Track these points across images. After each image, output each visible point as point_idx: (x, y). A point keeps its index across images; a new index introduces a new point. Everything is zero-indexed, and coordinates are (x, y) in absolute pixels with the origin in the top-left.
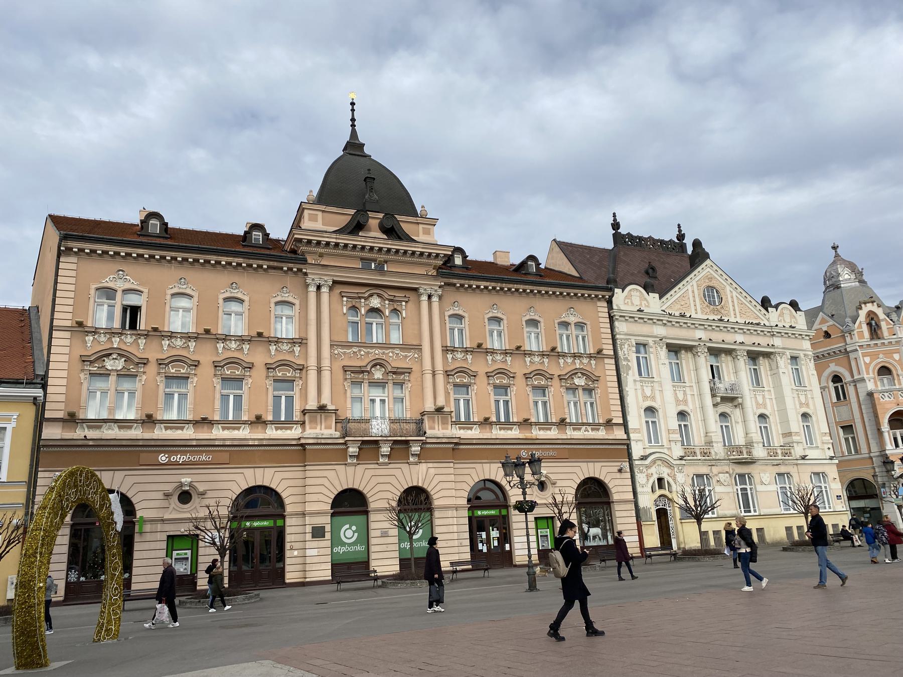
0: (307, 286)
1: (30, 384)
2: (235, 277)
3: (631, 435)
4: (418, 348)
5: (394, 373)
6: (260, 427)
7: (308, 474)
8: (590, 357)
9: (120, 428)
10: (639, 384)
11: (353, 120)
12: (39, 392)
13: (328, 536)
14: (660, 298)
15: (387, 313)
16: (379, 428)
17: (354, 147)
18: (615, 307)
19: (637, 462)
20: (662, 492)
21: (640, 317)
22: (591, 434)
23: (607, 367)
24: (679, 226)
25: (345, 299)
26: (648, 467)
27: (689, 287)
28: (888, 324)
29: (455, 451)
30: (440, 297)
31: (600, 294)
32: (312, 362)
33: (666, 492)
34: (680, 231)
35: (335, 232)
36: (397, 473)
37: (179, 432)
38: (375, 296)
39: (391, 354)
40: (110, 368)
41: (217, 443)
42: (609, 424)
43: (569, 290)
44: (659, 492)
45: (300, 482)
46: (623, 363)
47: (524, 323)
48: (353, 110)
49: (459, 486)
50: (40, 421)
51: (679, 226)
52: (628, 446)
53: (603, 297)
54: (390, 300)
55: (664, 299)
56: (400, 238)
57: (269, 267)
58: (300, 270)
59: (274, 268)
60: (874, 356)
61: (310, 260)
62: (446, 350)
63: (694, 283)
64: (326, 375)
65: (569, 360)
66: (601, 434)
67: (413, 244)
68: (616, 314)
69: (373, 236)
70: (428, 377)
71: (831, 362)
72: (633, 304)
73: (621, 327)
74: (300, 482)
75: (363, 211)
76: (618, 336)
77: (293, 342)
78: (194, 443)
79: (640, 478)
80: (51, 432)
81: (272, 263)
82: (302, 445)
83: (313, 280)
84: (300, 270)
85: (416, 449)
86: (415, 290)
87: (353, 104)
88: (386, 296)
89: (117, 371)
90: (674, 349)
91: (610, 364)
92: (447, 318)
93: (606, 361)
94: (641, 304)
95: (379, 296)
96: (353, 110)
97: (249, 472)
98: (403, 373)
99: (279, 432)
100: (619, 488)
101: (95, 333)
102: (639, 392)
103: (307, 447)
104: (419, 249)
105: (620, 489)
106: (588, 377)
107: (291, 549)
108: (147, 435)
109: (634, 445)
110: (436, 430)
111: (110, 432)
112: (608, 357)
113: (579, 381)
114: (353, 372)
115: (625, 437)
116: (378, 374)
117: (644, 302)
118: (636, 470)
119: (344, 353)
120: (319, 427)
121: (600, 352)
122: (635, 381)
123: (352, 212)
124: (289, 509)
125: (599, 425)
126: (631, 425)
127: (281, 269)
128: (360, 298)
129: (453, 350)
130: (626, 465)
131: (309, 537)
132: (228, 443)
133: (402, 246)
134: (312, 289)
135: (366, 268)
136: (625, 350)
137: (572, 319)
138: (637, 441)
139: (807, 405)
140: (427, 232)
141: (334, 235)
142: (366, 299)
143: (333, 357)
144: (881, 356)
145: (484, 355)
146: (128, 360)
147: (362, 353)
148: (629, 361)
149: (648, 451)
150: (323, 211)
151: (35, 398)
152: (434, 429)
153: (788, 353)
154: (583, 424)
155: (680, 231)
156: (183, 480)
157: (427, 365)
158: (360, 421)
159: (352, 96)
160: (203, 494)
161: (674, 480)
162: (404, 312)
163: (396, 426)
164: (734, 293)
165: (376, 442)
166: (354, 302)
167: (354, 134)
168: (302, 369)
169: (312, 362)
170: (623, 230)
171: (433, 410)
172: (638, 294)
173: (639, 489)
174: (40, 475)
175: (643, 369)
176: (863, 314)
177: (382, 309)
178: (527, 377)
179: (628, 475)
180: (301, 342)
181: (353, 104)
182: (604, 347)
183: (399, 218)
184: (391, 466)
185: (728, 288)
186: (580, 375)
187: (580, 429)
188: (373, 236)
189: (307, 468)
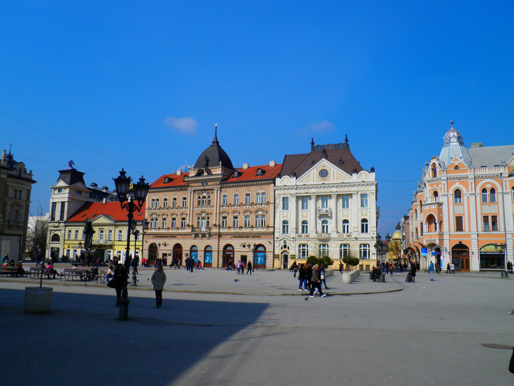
2: (174, 193)
20: (285, 249)
21: (285, 187)
24: (346, 135)
26: (280, 240)
27: (312, 172)
28: (439, 169)
33: (286, 249)
34: (346, 138)
42: (268, 227)
44: (284, 249)
46: (276, 205)
51: (346, 135)
55: (298, 179)
60: (432, 186)
63: (315, 170)
70: (215, 215)
71: (457, 182)
79: (277, 244)
90: (298, 198)
91: (272, 206)
100: (269, 248)
109: (276, 234)
130: (272, 242)
135: (203, 185)
139: (366, 215)
144: (435, 186)
153: (360, 193)
155: (346, 138)
159: (216, 125)
164: (335, 170)
169: (188, 213)
175: (285, 207)
176: (431, 163)
185: (332, 169)
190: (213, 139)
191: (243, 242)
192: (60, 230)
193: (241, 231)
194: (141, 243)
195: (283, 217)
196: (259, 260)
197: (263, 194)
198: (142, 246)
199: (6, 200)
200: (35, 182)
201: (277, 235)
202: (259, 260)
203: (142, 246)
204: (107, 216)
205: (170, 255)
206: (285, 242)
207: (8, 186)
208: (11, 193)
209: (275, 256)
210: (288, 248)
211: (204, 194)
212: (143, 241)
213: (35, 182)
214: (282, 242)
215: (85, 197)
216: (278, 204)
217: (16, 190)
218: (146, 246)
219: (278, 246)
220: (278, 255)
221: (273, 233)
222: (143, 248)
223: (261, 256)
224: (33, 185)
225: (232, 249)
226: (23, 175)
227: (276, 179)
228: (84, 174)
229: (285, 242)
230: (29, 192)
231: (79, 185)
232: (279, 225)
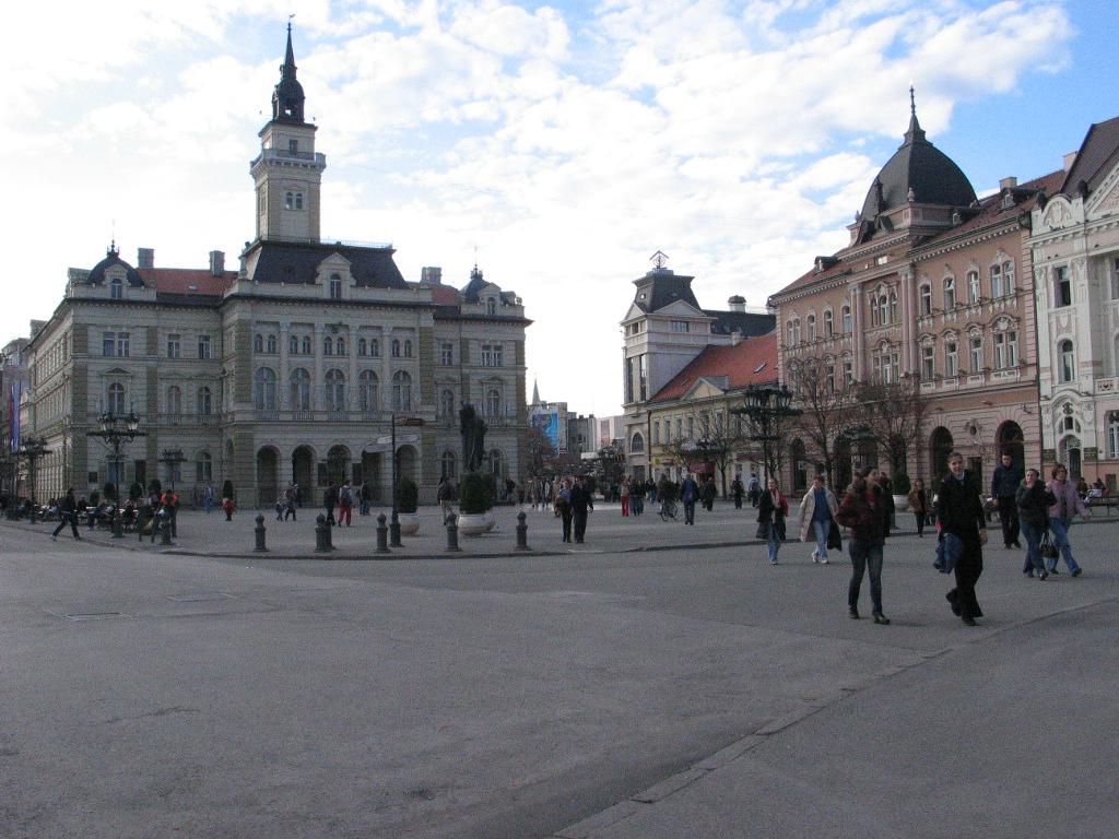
3: (1042, 376)
11: (913, 106)
14: (1084, 202)
20: (1070, 432)
26: (1056, 405)
33: (1073, 432)
42: (1023, 366)
44: (1066, 432)
48: (913, 97)
79: (1047, 419)
96: (913, 97)
109: (1042, 383)
142: (878, 291)
159: (911, 83)
161: (1082, 418)
167: (915, 121)
179: (1037, 416)
181: (912, 90)
190: (906, 127)
191: (969, 419)
192: (642, 424)
193: (963, 387)
195: (1059, 331)
199: (465, 371)
200: (529, 322)
201: (1045, 389)
204: (717, 381)
206: (1068, 410)
207: (467, 340)
208: (475, 353)
210: (1079, 431)
211: (884, 291)
213: (529, 322)
214: (1061, 409)
215: (703, 337)
217: (486, 347)
219: (1052, 420)
220: (1053, 451)
221: (1037, 382)
224: (527, 330)
226: (501, 312)
228: (690, 279)
229: (1068, 410)
230: (519, 347)
231: (678, 308)
232: (1048, 357)
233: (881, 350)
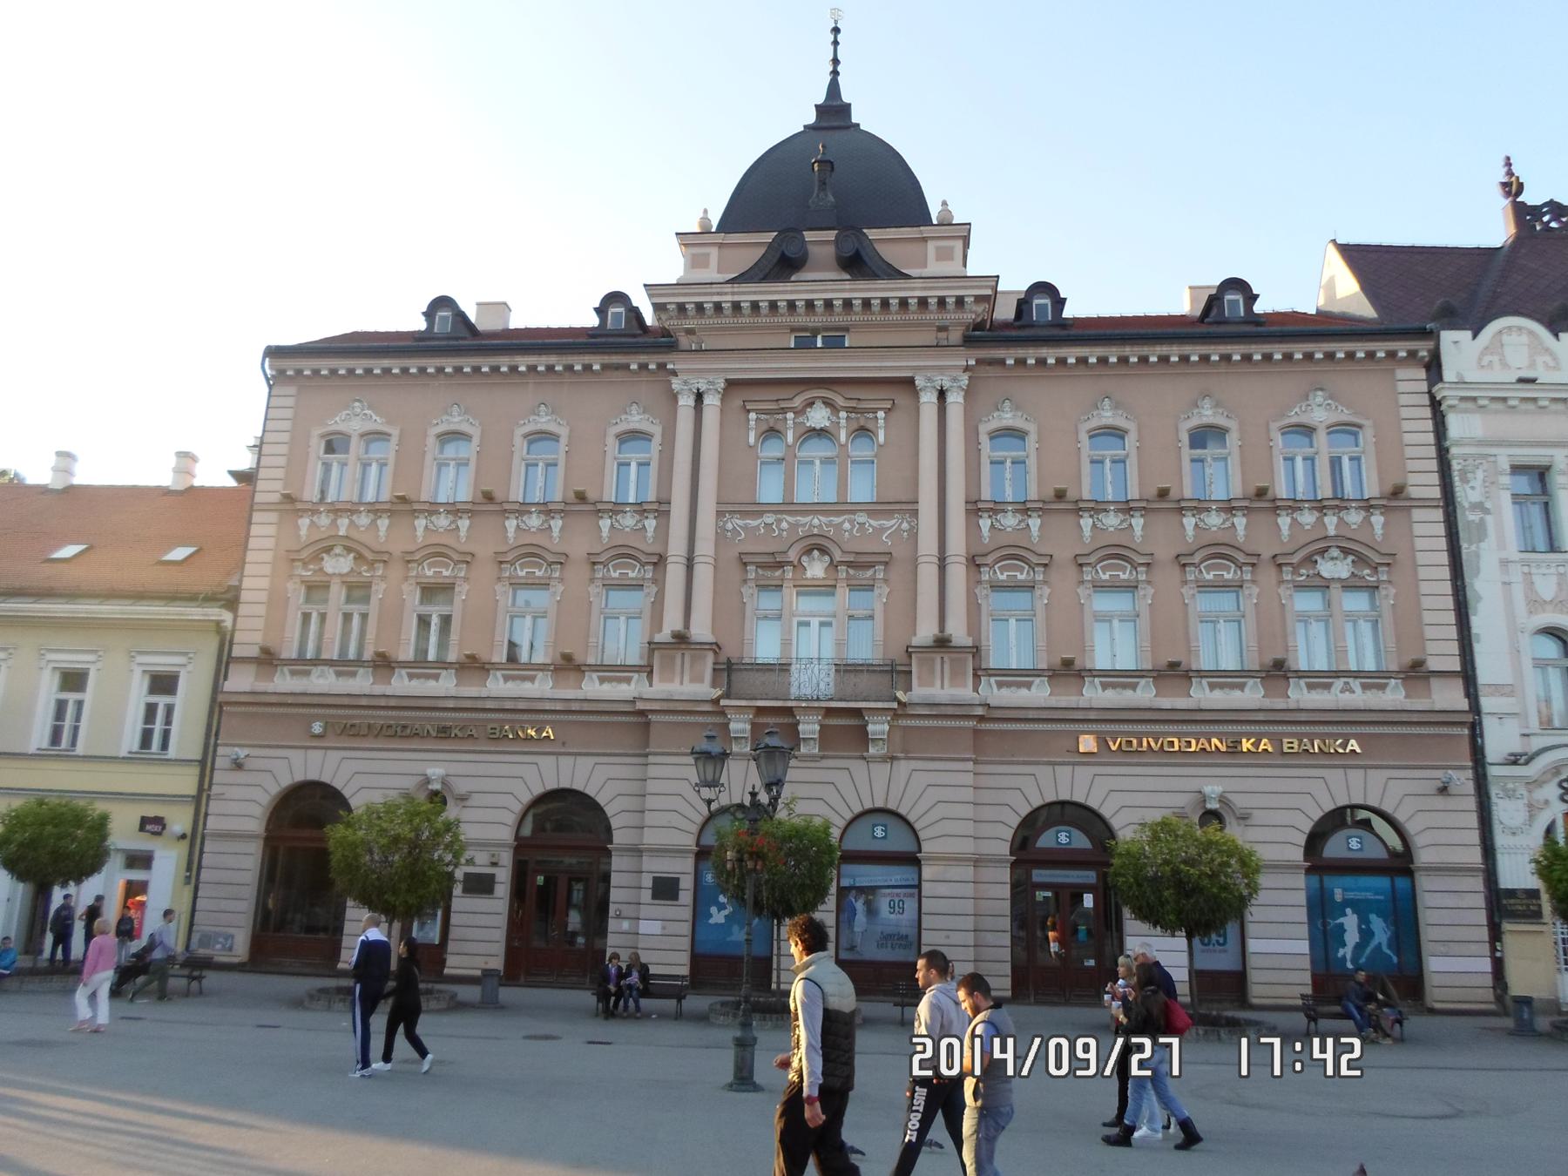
0: (674, 397)
1: (210, 599)
3: (1487, 703)
4: (910, 508)
5: (850, 564)
6: (573, 676)
7: (652, 771)
8: (1367, 506)
9: (339, 674)
10: (1516, 574)
11: (836, 61)
12: (227, 617)
13: (686, 897)
15: (843, 438)
16: (812, 680)
17: (834, 112)
18: (1449, 375)
19: (1493, 771)
22: (1358, 697)
23: (1418, 529)
25: (753, 416)
26: (1535, 783)
29: (987, 734)
30: (969, 393)
31: (1402, 348)
32: (676, 548)
35: (732, 281)
36: (841, 778)
37: (432, 683)
38: (819, 404)
39: (847, 526)
40: (329, 570)
41: (489, 705)
42: (1416, 673)
43: (1309, 347)
45: (633, 787)
46: (1467, 517)
47: (1185, 438)
48: (836, 43)
49: (988, 813)
50: (225, 662)
52: (1476, 730)
53: (1412, 354)
54: (849, 410)
56: (875, 276)
57: (605, 367)
58: (662, 366)
59: (618, 367)
61: (684, 342)
62: (974, 508)
64: (704, 575)
65: (1308, 518)
66: (1394, 696)
67: (901, 283)
68: (1441, 391)
69: (819, 284)
72: (1505, 365)
73: (1457, 426)
74: (633, 787)
75: (790, 232)
76: (1454, 451)
77: (641, 509)
78: (451, 704)
79: (1506, 812)
80: (241, 681)
81: (607, 359)
82: (642, 713)
83: (685, 383)
84: (662, 366)
85: (877, 727)
86: (910, 382)
87: (836, 30)
88: (840, 401)
89: (341, 575)
92: (984, 439)
93: (1417, 514)
94: (1532, 365)
95: (828, 403)
96: (836, 43)
97: (547, 763)
98: (871, 565)
99: (606, 687)
100: (1442, 836)
101: (353, 512)
102: (1518, 592)
103: (652, 717)
104: (913, 292)
105: (1443, 837)
106: (1360, 560)
107: (618, 917)
108: (379, 689)
109: (1490, 728)
110: (934, 687)
111: (321, 681)
112: (1424, 503)
113: (1335, 568)
114: (759, 566)
115: (1464, 704)
116: (816, 569)
117: (1541, 360)
118: (1494, 791)
119: (745, 528)
120: (677, 680)
121: (1398, 492)
122: (1505, 563)
123: (769, 237)
124: (619, 838)
125: (1387, 675)
126: (1484, 675)
127: (627, 367)
128: (784, 411)
129: (996, 508)
130: (1463, 780)
131: (646, 895)
132: (508, 705)
133: (876, 290)
134: (686, 401)
136: (1478, 483)
137: (1319, 414)
138: (1501, 717)
140: (944, 255)
141: (728, 288)
142: (799, 412)
143: (721, 536)
145: (1071, 518)
146: (359, 557)
147: (784, 525)
148: (1487, 511)
149: (1537, 743)
150: (721, 245)
151: (218, 623)
152: (932, 685)
154: (1337, 674)
156: (429, 771)
157: (928, 543)
158: (767, 668)
160: (462, 799)
162: (881, 438)
163: (853, 679)
165: (789, 711)
166: (772, 420)
167: (834, 89)
168: (660, 562)
169: (676, 548)
170: (1531, 197)
171: (929, 641)
172: (1525, 339)
173: (1501, 840)
174: (220, 750)
177: (833, 431)
178: (1182, 562)
179: (1471, 803)
180: (661, 509)
181: (836, 30)
182: (1412, 479)
183: (872, 234)
184: (825, 763)
186: (1335, 552)
187: (1328, 687)
188: (819, 284)
189: (651, 759)
190: (821, 100)
193: (1181, 703)
194: (186, 783)
196: (1352, 937)
197: (1349, 429)
198: (200, 799)
201: (1499, 740)
202: (1352, 937)
203: (200, 799)
205: (480, 885)
209: (1503, 907)
212: (205, 765)
216: (1478, 506)
218: (244, 807)
222: (199, 817)
223: (1362, 909)
225: (1081, 841)
227: (1447, 337)
233: (799, 567)
